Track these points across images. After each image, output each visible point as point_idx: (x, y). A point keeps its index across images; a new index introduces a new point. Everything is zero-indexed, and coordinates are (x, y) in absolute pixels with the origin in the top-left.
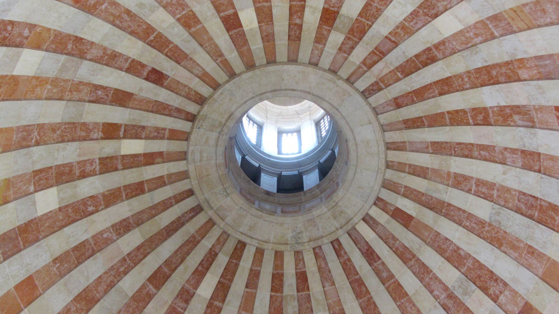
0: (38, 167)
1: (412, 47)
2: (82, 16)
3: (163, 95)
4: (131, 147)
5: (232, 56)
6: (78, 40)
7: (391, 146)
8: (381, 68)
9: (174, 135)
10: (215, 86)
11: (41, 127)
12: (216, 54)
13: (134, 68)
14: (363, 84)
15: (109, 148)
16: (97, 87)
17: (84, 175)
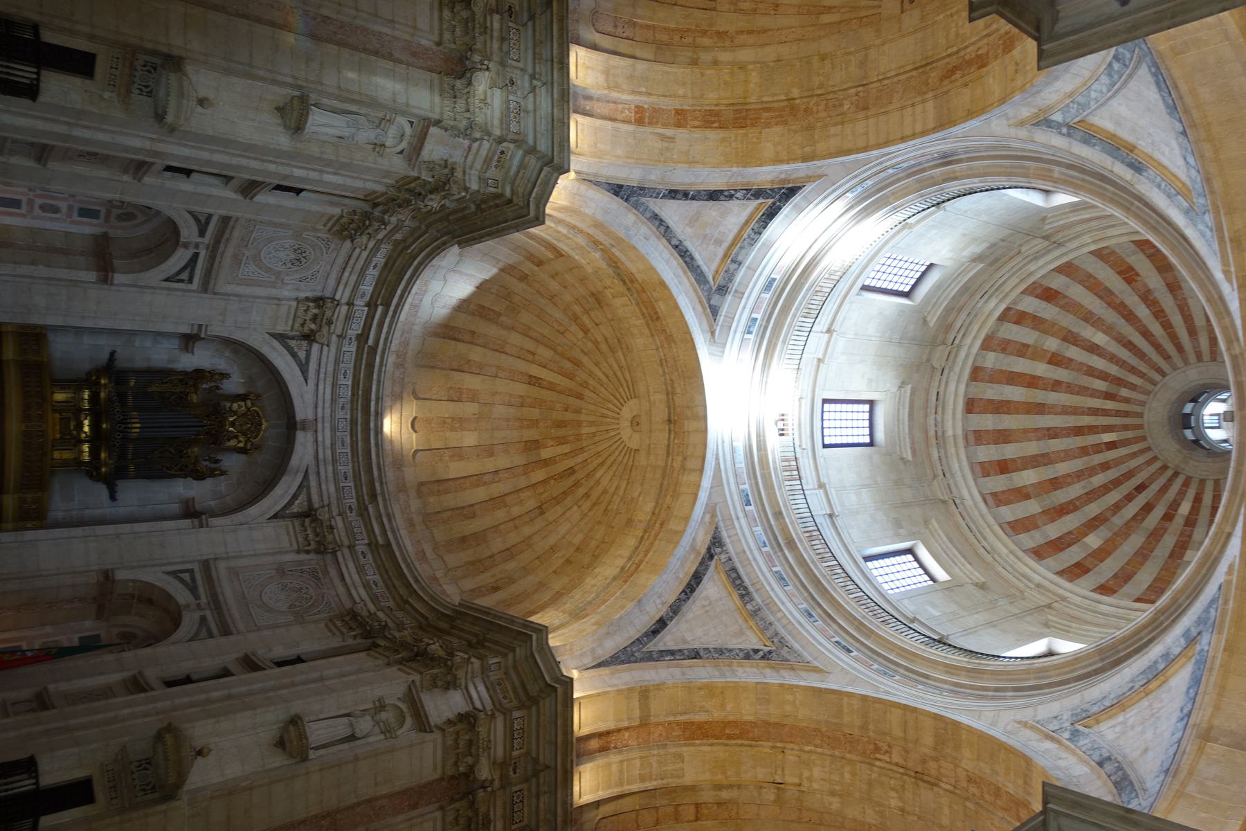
0: (1167, 555)
1: (1124, 354)
2: (1077, 513)
3: (1155, 487)
4: (1185, 508)
5: (1135, 448)
6: (1095, 519)
7: (1199, 357)
8: (1143, 368)
9: (1186, 484)
10: (1155, 458)
11: (1142, 548)
12: (1134, 455)
13: (1129, 498)
14: (1157, 377)
15: (1179, 521)
16: (1134, 518)
17: (1190, 536)
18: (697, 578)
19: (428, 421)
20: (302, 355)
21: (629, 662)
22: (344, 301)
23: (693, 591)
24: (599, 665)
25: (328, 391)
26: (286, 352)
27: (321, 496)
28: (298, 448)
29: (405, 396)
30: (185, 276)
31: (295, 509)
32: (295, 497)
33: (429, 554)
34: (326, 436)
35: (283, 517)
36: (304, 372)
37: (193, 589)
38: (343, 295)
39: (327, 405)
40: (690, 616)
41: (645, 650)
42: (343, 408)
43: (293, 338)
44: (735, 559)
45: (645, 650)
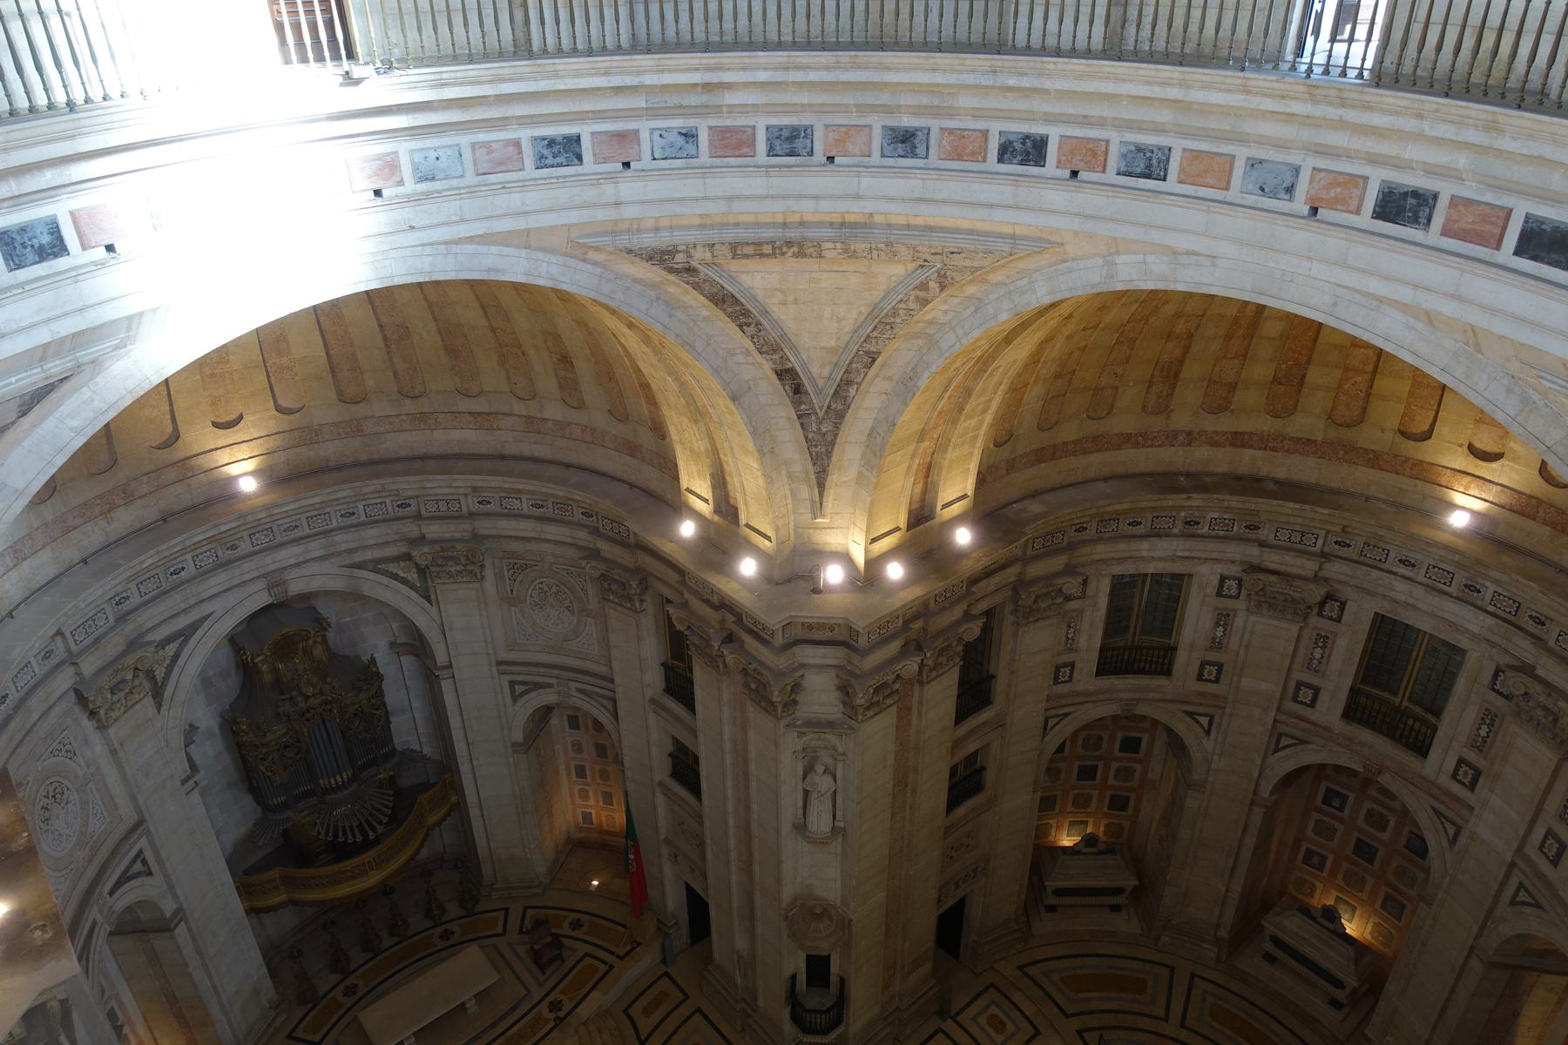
18: (722, 299)
19: (215, 402)
20: (171, 649)
21: (833, 444)
22: (71, 670)
23: (746, 313)
24: (821, 486)
25: (213, 581)
26: (176, 670)
27: (386, 544)
28: (315, 585)
29: (178, 452)
30: (138, 867)
31: (413, 576)
32: (395, 577)
33: (479, 405)
34: (287, 556)
35: (427, 589)
36: (194, 627)
37: (538, 686)
38: (64, 681)
39: (237, 572)
40: (790, 326)
41: (821, 414)
42: (233, 548)
43: (153, 679)
44: (714, 236)
45: (821, 414)
